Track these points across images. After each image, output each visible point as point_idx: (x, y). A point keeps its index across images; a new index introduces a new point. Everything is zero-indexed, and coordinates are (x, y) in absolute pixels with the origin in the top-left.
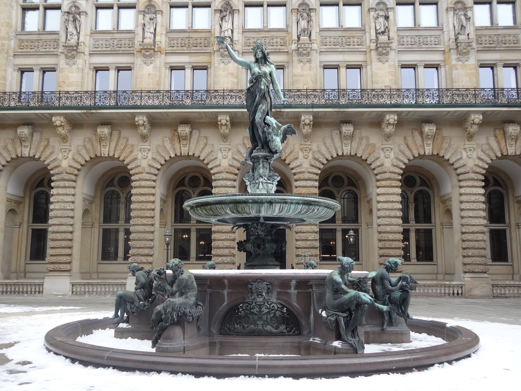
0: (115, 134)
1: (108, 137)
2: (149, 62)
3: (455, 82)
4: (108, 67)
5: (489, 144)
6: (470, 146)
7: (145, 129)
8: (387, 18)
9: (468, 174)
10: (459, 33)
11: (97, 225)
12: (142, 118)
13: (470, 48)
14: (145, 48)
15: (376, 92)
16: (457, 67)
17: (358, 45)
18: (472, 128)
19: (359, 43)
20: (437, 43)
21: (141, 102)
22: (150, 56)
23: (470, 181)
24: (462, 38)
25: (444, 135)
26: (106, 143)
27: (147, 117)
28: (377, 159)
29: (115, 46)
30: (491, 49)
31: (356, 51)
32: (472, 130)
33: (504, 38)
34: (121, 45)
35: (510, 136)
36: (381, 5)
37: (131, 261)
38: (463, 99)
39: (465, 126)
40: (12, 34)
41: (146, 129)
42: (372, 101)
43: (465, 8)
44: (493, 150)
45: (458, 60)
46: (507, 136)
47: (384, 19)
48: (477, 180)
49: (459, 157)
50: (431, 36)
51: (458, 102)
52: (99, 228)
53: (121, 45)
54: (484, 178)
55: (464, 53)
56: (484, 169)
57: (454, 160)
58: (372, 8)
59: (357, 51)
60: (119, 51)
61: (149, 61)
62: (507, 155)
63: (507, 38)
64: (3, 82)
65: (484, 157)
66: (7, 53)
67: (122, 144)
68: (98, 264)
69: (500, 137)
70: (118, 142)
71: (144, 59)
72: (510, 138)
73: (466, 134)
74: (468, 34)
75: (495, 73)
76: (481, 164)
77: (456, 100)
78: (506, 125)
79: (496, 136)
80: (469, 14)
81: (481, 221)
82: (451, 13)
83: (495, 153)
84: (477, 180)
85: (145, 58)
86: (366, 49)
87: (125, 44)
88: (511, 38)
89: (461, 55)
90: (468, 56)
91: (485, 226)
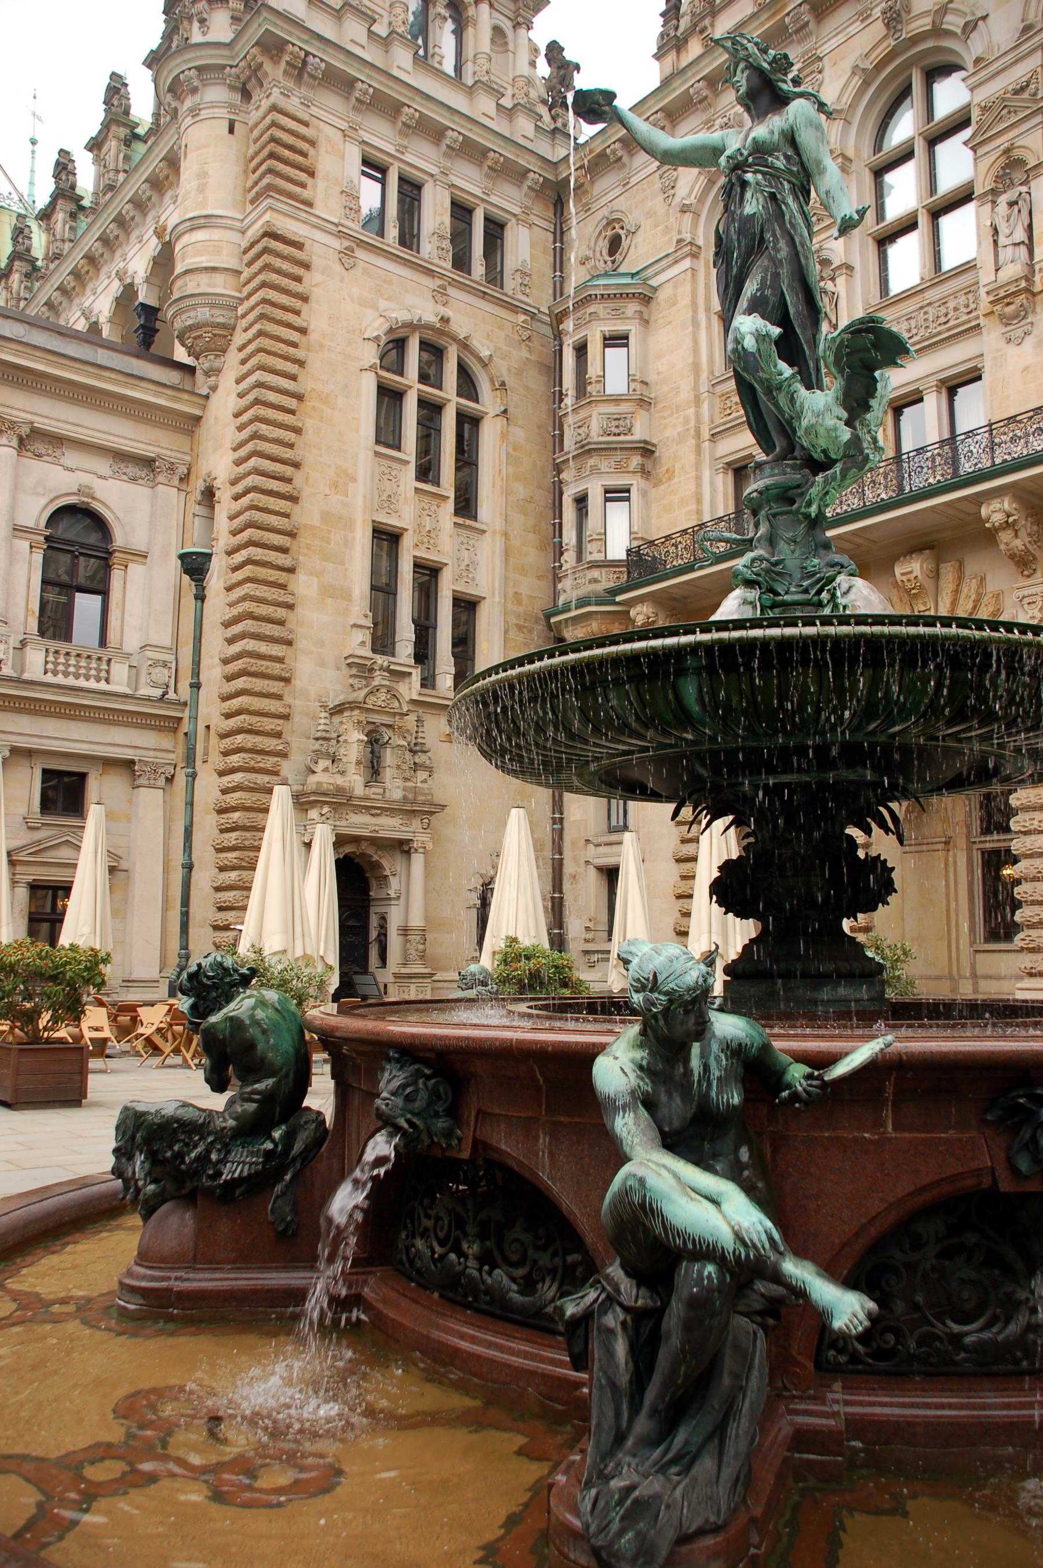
0: (948, 572)
1: (929, 584)
2: (1020, 332)
4: (918, 391)
7: (1016, 536)
11: (961, 842)
12: (998, 506)
14: (1002, 293)
21: (993, 458)
22: (1021, 314)
26: (925, 604)
27: (1017, 498)
29: (932, 325)
34: (946, 315)
37: (1022, 944)
40: (704, 387)
41: (1022, 533)
52: (969, 850)
53: (946, 315)
60: (939, 333)
61: (1020, 331)
64: (694, 507)
66: (698, 435)
67: (968, 597)
68: (976, 951)
70: (957, 592)
71: (1005, 330)
85: (1007, 325)
87: (956, 309)
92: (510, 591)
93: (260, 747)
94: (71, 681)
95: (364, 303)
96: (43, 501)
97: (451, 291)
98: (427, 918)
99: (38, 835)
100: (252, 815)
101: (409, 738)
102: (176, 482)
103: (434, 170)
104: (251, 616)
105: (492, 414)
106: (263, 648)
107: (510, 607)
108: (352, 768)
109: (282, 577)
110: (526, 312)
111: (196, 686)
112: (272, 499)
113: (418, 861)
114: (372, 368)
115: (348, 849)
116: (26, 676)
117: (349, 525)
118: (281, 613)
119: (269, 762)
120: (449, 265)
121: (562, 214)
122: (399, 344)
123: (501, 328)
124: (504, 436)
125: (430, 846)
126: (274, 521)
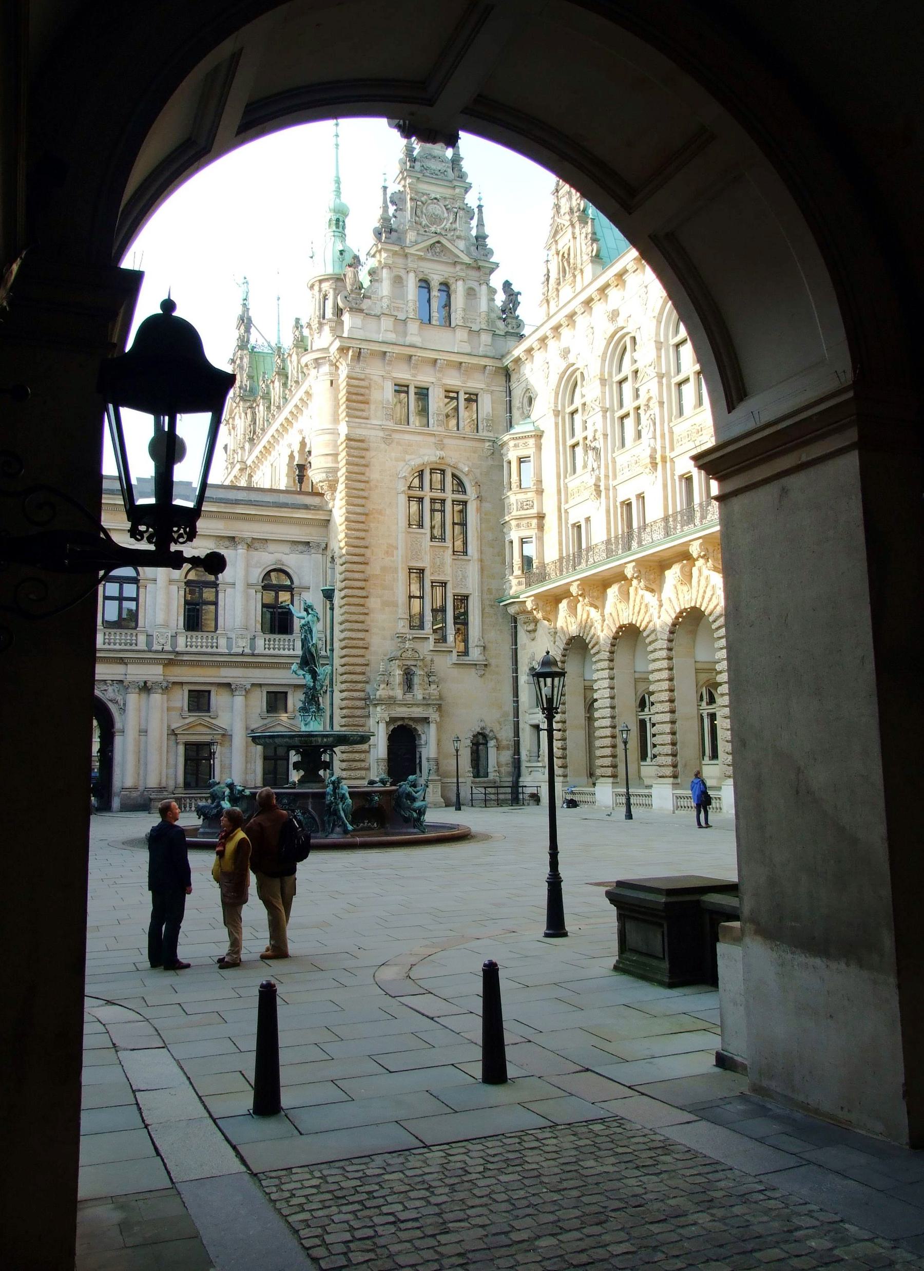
92: (485, 589)
93: (355, 680)
94: (276, 652)
95: (397, 460)
96: (260, 570)
97: (446, 441)
98: (439, 753)
99: (265, 722)
100: (353, 710)
101: (426, 670)
102: (321, 551)
103: (433, 380)
104: (347, 621)
105: (473, 498)
106: (353, 634)
107: (485, 596)
108: (397, 687)
109: (361, 601)
110: (489, 441)
111: (332, 650)
112: (355, 566)
113: (433, 727)
114: (403, 492)
115: (399, 723)
116: (256, 652)
117: (395, 570)
118: (361, 618)
119: (359, 686)
120: (443, 430)
121: (510, 381)
122: (421, 474)
123: (474, 452)
124: (479, 510)
125: (438, 720)
126: (357, 576)
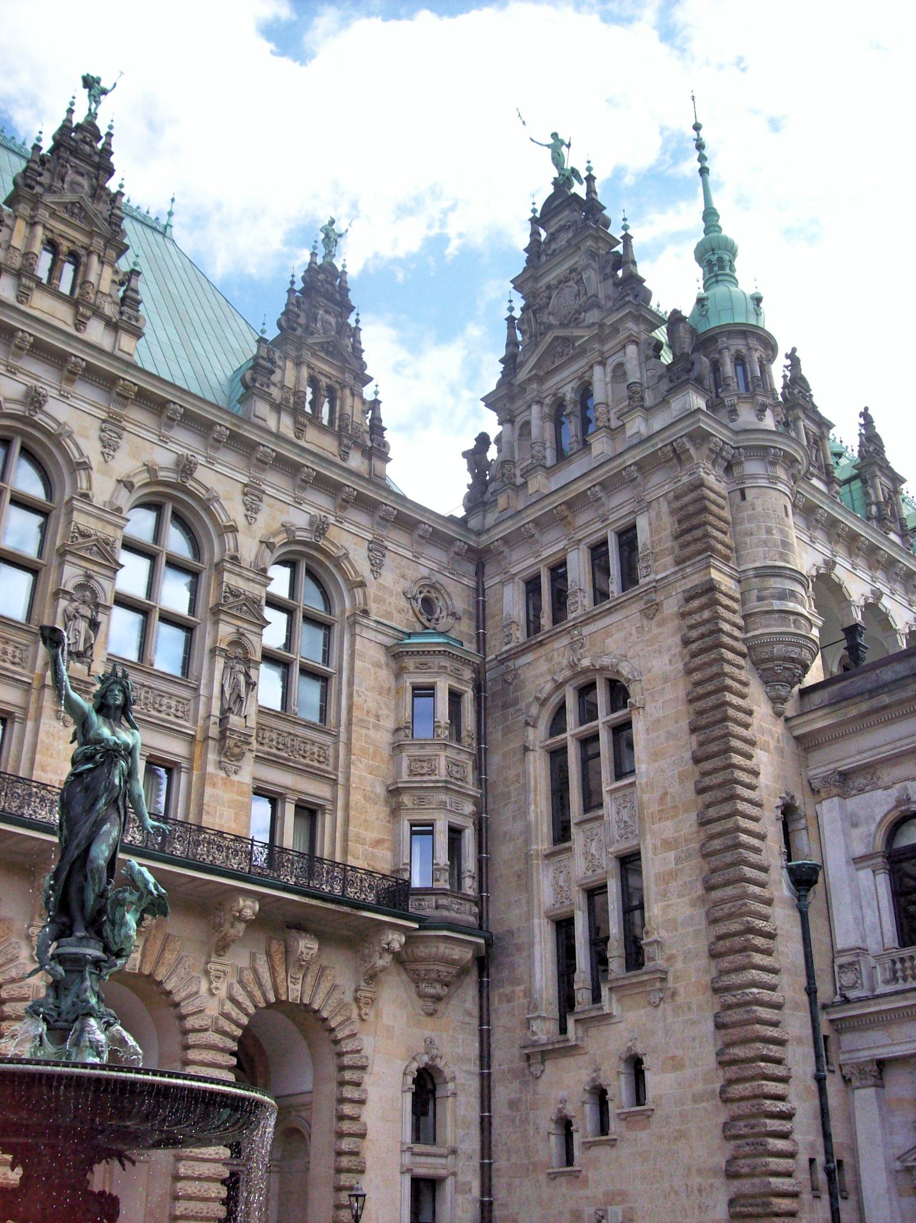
3: (208, 813)
5: (255, 971)
6: (220, 968)
8: (94, 625)
9: (207, 1033)
10: (230, 709)
13: (245, 747)
15: (50, 792)
16: (215, 780)
17: (13, 663)
18: (232, 926)
19: (17, 660)
20: (180, 714)
23: (207, 1051)
24: (234, 720)
25: (169, 931)
28: (12, 960)
30: (281, 761)
31: (7, 676)
32: (232, 932)
33: (303, 745)
35: (299, 960)
36: (88, 593)
38: (227, 857)
39: (218, 920)
42: (35, 812)
43: (248, 661)
44: (260, 984)
45: (220, 765)
46: (292, 959)
47: (87, 625)
48: (223, 1050)
49: (195, 990)
50: (171, 696)
51: (218, 862)
54: (236, 1048)
55: (233, 755)
56: (238, 1025)
57: (183, 994)
58: (66, 592)
59: (9, 677)
62: (287, 1001)
63: (308, 747)
65: (242, 997)
69: (278, 958)
72: (297, 964)
73: (214, 940)
74: (245, 717)
75: (279, 814)
76: (235, 1013)
77: (214, 858)
78: (293, 932)
79: (269, 955)
80: (252, 672)
81: (221, 1151)
82: (220, 663)
83: (264, 994)
84: (223, 1050)
86: (32, 679)
88: (316, 749)
89: (226, 756)
90: (239, 764)
91: (224, 1164)
